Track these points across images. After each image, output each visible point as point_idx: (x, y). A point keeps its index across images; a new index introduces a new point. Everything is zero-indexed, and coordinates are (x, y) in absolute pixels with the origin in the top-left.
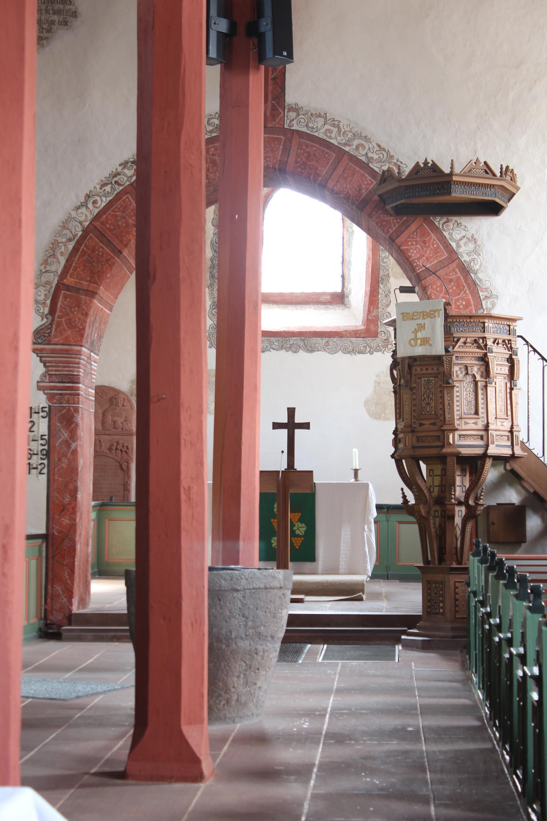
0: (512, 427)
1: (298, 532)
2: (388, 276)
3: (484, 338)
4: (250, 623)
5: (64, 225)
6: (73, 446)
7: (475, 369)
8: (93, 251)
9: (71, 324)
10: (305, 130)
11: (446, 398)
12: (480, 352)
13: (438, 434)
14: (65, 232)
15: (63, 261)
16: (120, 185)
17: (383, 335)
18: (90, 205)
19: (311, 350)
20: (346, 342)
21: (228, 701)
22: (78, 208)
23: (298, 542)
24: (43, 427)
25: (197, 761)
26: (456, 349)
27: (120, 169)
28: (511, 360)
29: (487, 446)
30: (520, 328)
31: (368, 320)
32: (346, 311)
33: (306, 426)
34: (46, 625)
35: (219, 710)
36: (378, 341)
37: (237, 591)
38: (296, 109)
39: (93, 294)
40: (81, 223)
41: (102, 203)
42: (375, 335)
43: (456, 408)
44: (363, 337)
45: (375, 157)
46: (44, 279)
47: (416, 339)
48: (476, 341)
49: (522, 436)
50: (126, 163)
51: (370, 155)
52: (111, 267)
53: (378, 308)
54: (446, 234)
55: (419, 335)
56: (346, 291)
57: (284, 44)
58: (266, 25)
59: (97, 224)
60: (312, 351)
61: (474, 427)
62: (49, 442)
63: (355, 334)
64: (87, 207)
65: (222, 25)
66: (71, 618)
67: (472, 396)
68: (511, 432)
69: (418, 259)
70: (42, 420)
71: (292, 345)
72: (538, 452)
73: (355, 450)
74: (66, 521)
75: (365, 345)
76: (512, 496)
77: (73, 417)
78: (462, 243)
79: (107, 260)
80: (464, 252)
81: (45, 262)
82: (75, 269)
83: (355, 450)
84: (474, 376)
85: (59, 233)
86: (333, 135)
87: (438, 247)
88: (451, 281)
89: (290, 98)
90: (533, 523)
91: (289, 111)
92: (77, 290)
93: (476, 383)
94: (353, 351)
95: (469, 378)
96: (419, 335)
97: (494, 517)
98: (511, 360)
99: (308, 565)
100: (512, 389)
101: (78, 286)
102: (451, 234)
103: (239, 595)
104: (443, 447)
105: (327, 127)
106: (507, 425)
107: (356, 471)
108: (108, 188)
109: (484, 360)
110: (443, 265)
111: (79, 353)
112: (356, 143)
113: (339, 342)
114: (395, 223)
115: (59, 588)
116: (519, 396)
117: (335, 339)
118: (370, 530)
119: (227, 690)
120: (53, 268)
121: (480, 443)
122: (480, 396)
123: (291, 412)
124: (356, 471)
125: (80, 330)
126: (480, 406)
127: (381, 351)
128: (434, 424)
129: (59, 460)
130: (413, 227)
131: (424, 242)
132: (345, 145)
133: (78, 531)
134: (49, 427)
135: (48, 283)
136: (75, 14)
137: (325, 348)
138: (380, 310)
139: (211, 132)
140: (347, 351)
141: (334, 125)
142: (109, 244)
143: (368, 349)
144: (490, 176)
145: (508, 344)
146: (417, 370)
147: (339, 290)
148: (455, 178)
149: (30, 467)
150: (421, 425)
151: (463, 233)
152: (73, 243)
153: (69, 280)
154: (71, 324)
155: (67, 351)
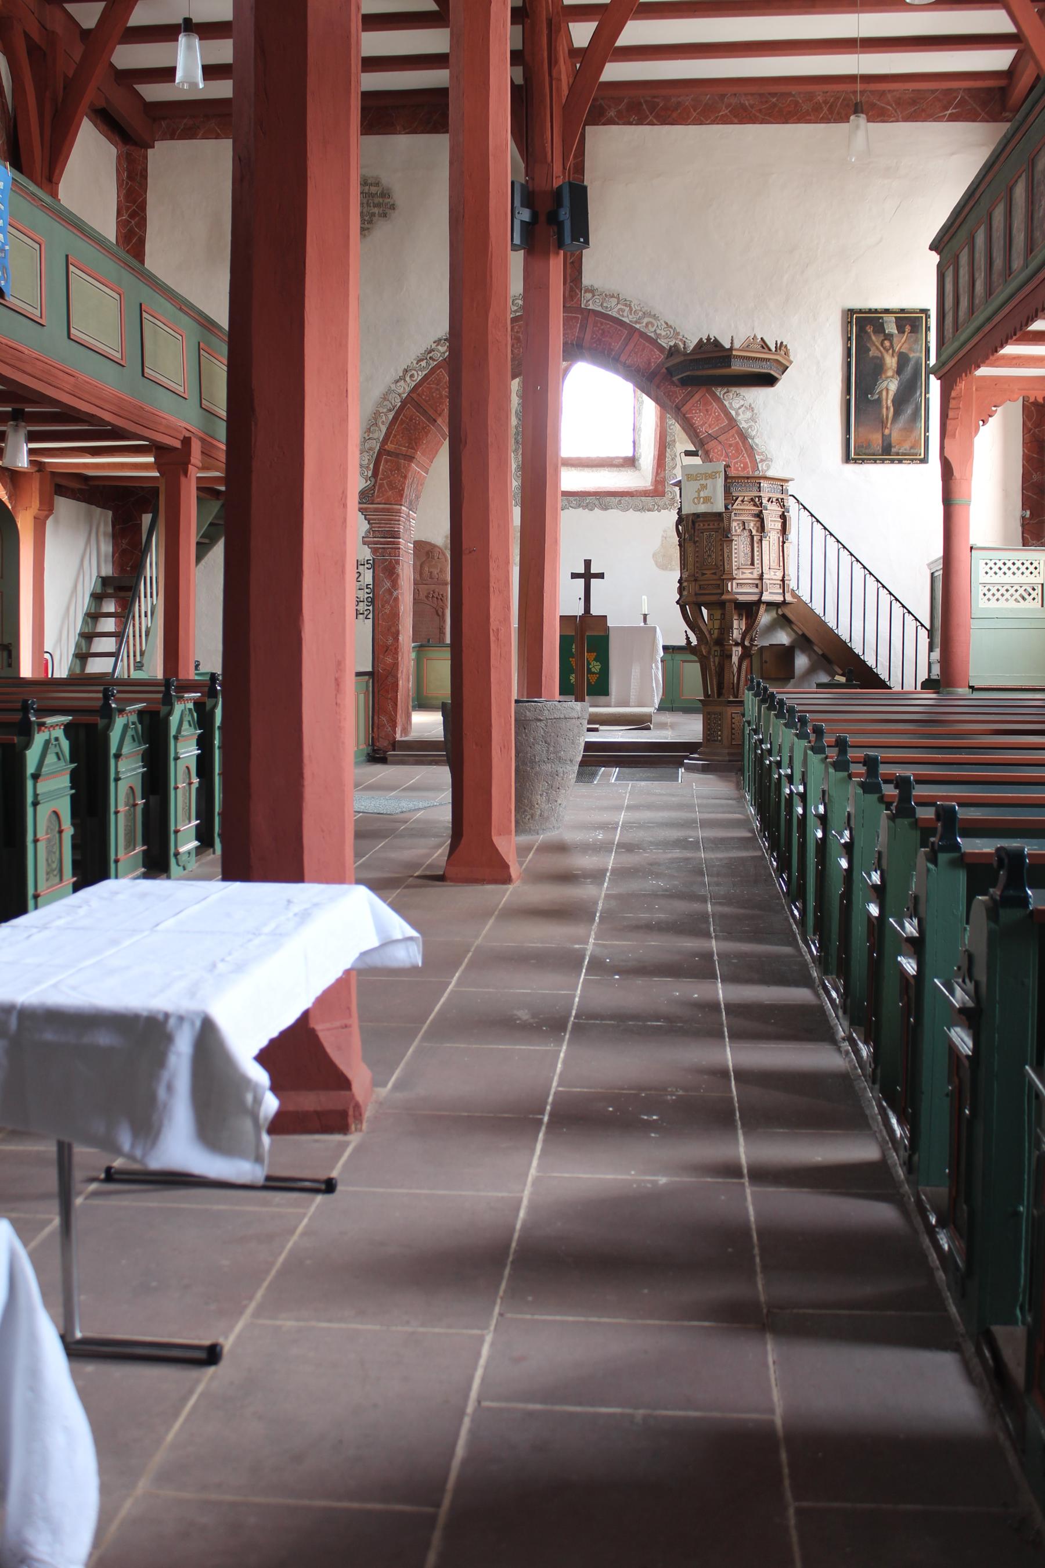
0: (784, 577)
1: (593, 670)
2: (674, 441)
3: (760, 497)
4: (551, 749)
5: (385, 397)
6: (395, 593)
7: (752, 524)
8: (411, 420)
9: (391, 486)
10: (599, 309)
11: (726, 550)
12: (756, 510)
13: (718, 582)
14: (386, 403)
15: (384, 429)
16: (434, 360)
18: (408, 379)
19: (605, 508)
20: (637, 501)
21: (532, 816)
22: (397, 382)
23: (594, 679)
24: (368, 577)
25: (506, 867)
26: (735, 507)
27: (434, 346)
28: (783, 517)
29: (762, 593)
30: (791, 488)
33: (601, 576)
34: (374, 750)
35: (525, 823)
36: (666, 500)
37: (540, 720)
38: (592, 290)
39: (411, 458)
40: (399, 395)
41: (419, 376)
42: (662, 494)
43: (734, 560)
45: (663, 333)
46: (367, 446)
47: (699, 498)
48: (752, 500)
49: (792, 584)
50: (440, 340)
51: (658, 332)
52: (427, 434)
54: (726, 403)
55: (702, 494)
56: (637, 456)
57: (581, 231)
58: (565, 214)
59: (414, 396)
60: (606, 509)
61: (750, 576)
62: (373, 591)
63: (645, 493)
64: (405, 380)
65: (525, 215)
66: (395, 745)
67: (749, 549)
68: (783, 580)
69: (702, 426)
70: (367, 571)
71: (588, 504)
72: (806, 598)
73: (644, 597)
74: (389, 660)
76: (783, 638)
77: (394, 568)
78: (740, 411)
79: (424, 428)
80: (743, 419)
81: (369, 431)
82: (395, 436)
83: (644, 597)
84: (750, 531)
85: (380, 404)
86: (625, 314)
87: (719, 415)
88: (730, 445)
89: (587, 280)
90: (801, 662)
91: (586, 292)
92: (397, 455)
93: (752, 537)
94: (642, 509)
95: (746, 533)
96: (702, 494)
97: (766, 656)
98: (783, 517)
99: (602, 699)
100: (784, 542)
101: (398, 452)
102: (731, 404)
103: (542, 724)
104: (722, 594)
105: (619, 306)
106: (780, 575)
107: (645, 616)
108: (423, 363)
109: (760, 516)
110: (724, 431)
111: (399, 511)
112: (645, 320)
114: (680, 393)
115: (384, 719)
116: (790, 549)
118: (657, 668)
119: (532, 807)
120: (376, 436)
121: (756, 590)
122: (756, 549)
123: (588, 563)
124: (645, 616)
125: (400, 491)
126: (756, 557)
128: (715, 574)
129: (383, 606)
130: (697, 397)
131: (707, 411)
132: (636, 322)
133: (400, 669)
134: (374, 577)
135: (371, 449)
136: (393, 207)
137: (617, 507)
139: (515, 311)
140: (637, 509)
141: (626, 305)
142: (425, 413)
144: (766, 350)
145: (781, 502)
146: (700, 525)
147: (630, 454)
148: (734, 353)
149: (358, 613)
150: (703, 574)
151: (742, 402)
152: (393, 413)
153: (390, 447)
154: (391, 486)
155: (388, 510)
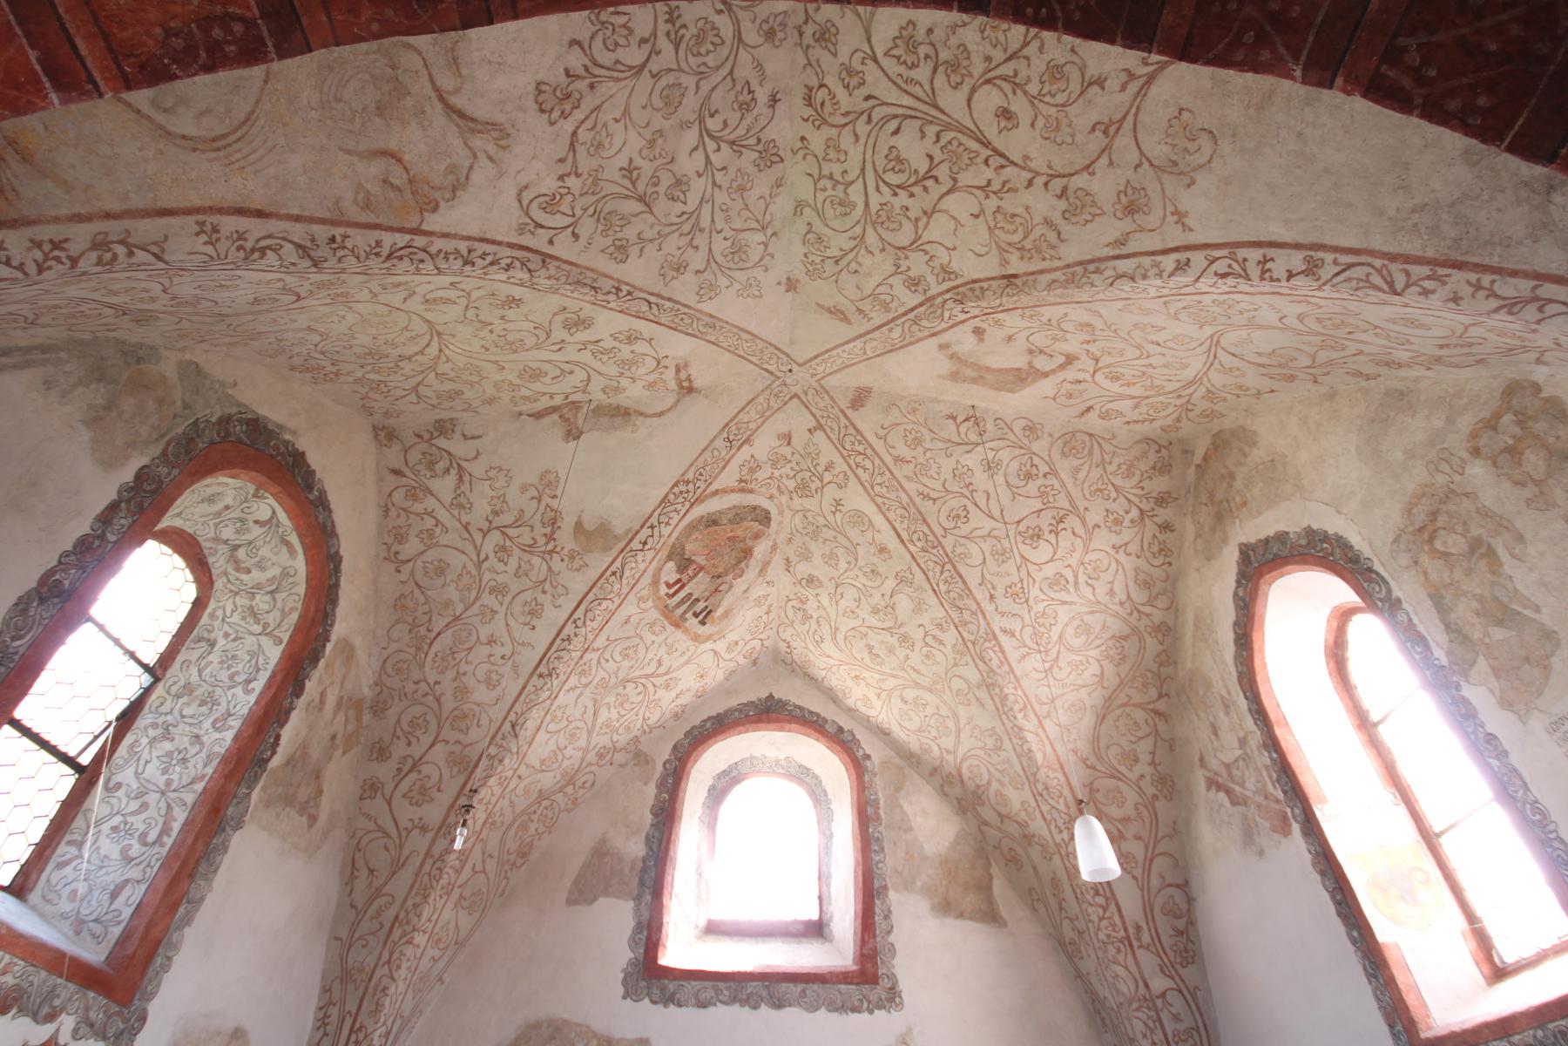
2: (885, 887)
19: (779, 1004)
20: (833, 991)
31: (862, 955)
32: (827, 946)
36: (879, 991)
53: (875, 936)
56: (826, 918)
63: (843, 977)
71: (749, 996)
113: (821, 991)
117: (815, 986)
147: (815, 916)
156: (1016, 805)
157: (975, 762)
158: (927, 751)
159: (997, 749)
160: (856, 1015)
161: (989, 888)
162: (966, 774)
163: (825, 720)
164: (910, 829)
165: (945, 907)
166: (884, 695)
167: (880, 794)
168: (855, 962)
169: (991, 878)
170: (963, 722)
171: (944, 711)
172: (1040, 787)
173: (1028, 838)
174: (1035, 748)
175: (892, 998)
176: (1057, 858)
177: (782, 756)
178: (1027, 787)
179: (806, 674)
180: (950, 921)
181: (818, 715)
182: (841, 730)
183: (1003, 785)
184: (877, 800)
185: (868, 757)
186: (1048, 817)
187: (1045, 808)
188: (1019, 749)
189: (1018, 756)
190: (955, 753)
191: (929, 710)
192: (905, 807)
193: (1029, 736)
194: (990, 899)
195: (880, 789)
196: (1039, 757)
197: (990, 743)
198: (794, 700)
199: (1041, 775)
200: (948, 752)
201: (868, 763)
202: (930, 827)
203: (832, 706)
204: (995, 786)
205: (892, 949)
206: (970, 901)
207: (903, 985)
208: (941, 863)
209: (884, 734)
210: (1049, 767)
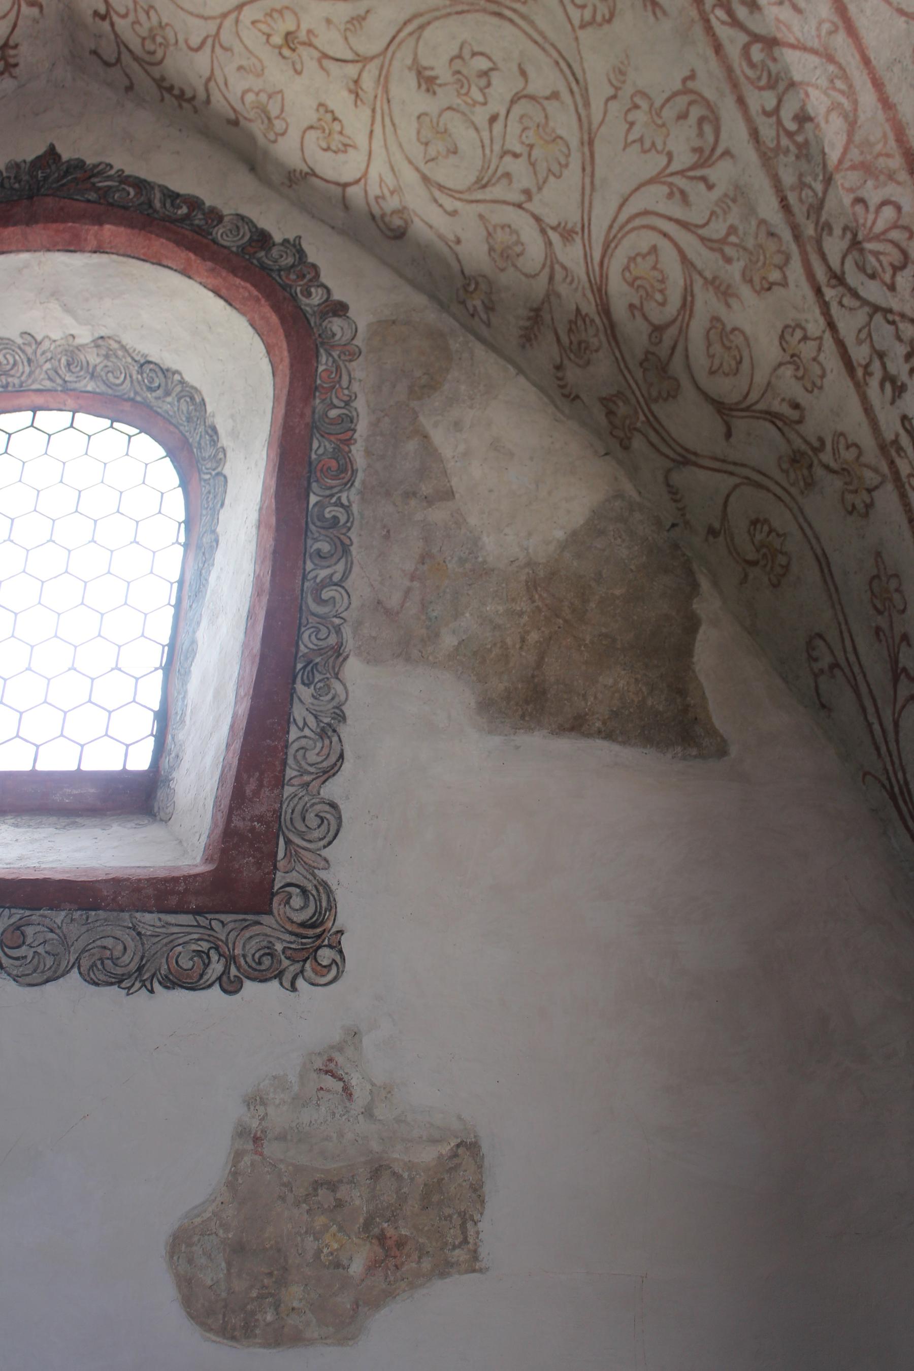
17: (297, 902)
20: (114, 933)
32: (153, 831)
44: (197, 912)
53: (280, 782)
63: (161, 894)
75: (205, 946)
113: (73, 930)
117: (60, 917)
127: (279, 975)
138: (288, 791)
143: (217, 967)
147: (141, 760)
156: (767, 350)
157: (644, 240)
158: (507, 255)
159: (705, 157)
160: (180, 996)
161: (684, 652)
162: (618, 290)
163: (215, 216)
164: (449, 494)
165: (528, 702)
166: (368, 83)
167: (360, 404)
168: (208, 860)
169: (692, 625)
170: (599, 92)
171: (545, 79)
172: (834, 247)
173: (802, 460)
174: (818, 102)
175: (314, 948)
176: (887, 500)
177: (84, 336)
178: (795, 270)
179: (164, 87)
180: (535, 741)
181: (194, 203)
182: (262, 239)
183: (725, 293)
184: (348, 421)
185: (340, 309)
186: (860, 354)
187: (849, 324)
188: (768, 132)
189: (767, 158)
190: (585, 227)
191: (502, 88)
192: (438, 436)
193: (799, 65)
194: (680, 684)
195: (363, 389)
196: (832, 135)
197: (681, 143)
198: (123, 162)
199: (840, 199)
200: (567, 235)
201: (336, 325)
202: (515, 482)
203: (243, 180)
204: (706, 303)
205: (332, 821)
206: (616, 682)
207: (350, 914)
208: (532, 585)
209: (385, 235)
210: (867, 169)
